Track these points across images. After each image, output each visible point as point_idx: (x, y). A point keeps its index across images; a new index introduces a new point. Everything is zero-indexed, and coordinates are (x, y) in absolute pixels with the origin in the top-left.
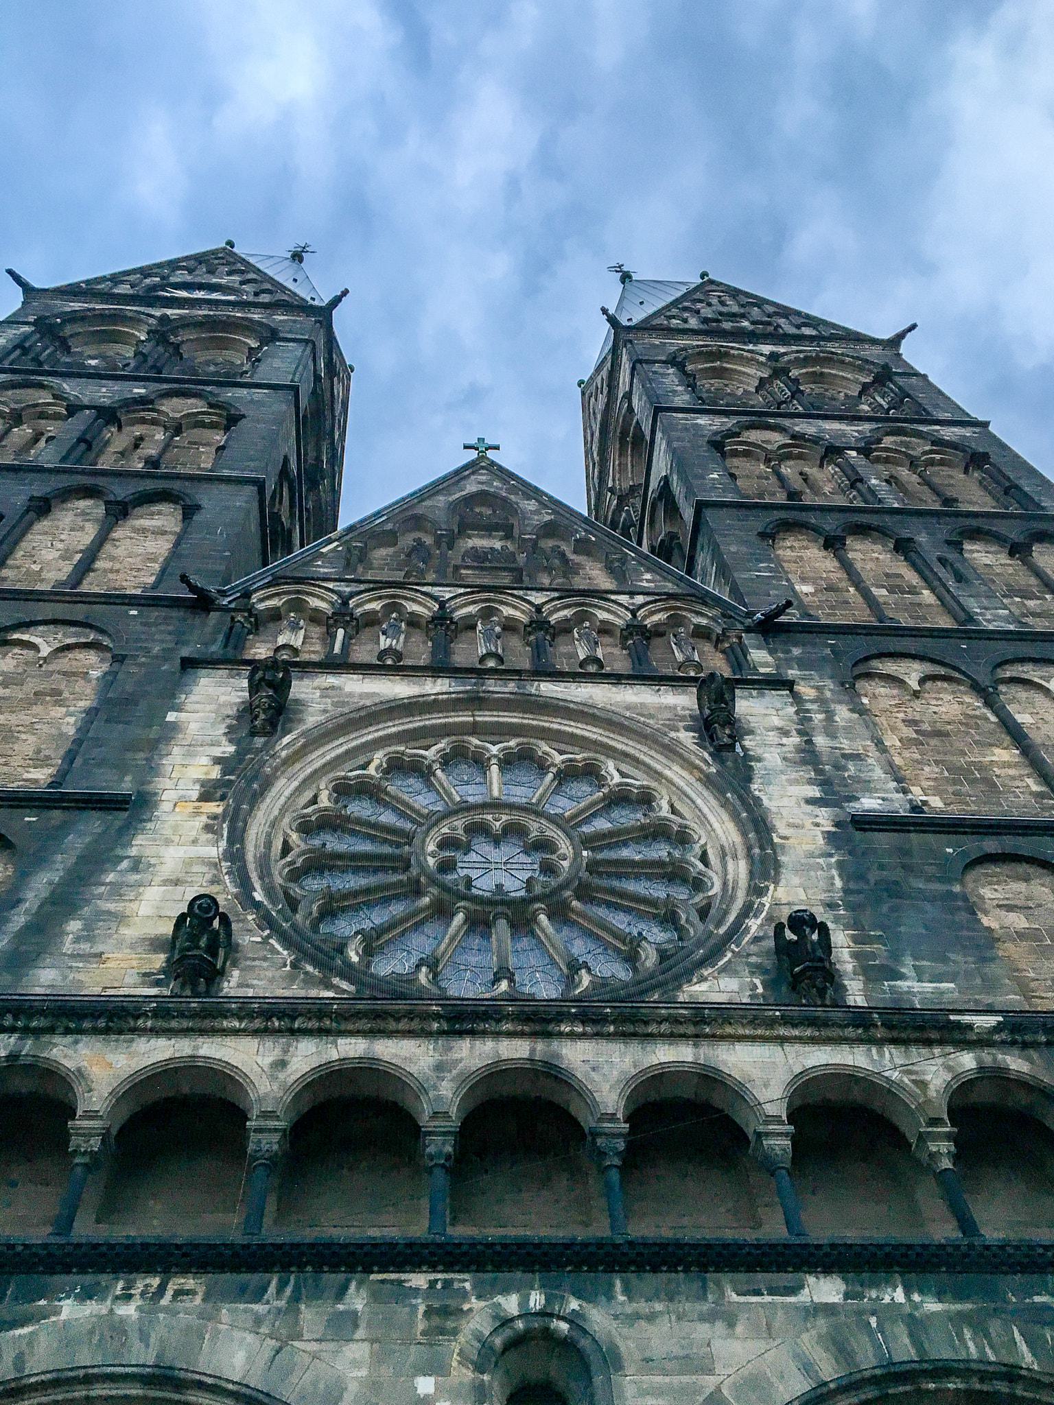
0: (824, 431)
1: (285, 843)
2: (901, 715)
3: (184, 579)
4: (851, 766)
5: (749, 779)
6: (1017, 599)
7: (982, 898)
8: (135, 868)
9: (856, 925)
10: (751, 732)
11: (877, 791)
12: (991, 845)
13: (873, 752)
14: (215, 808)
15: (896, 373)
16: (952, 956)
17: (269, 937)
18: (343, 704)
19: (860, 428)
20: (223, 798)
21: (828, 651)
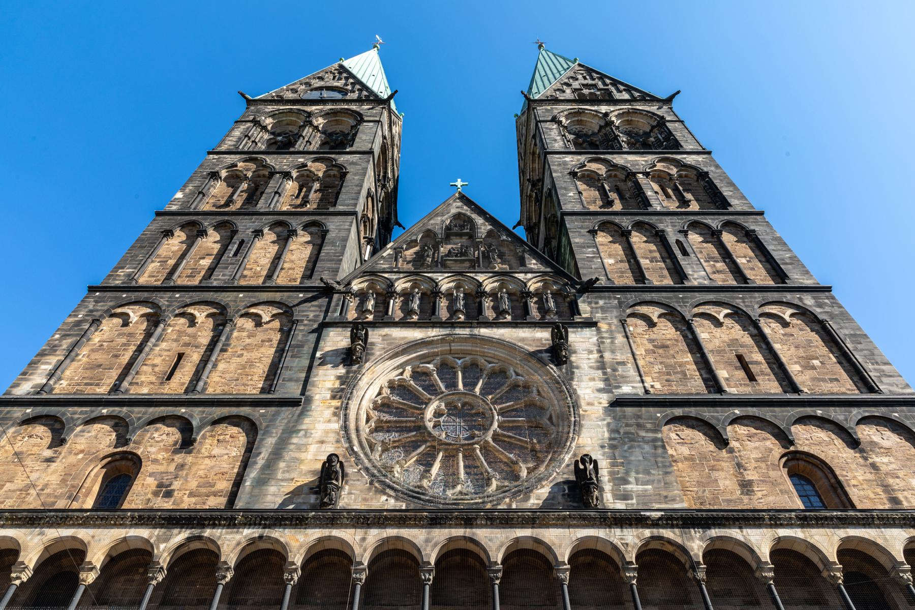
0: (628, 162)
1: (367, 415)
2: (647, 336)
3: (321, 279)
4: (620, 369)
5: (572, 379)
6: (712, 263)
7: (670, 439)
8: (305, 436)
10: (575, 352)
11: (631, 382)
14: (336, 403)
15: (669, 121)
16: (653, 472)
17: (360, 469)
18: (391, 343)
19: (646, 159)
20: (340, 398)
21: (616, 302)
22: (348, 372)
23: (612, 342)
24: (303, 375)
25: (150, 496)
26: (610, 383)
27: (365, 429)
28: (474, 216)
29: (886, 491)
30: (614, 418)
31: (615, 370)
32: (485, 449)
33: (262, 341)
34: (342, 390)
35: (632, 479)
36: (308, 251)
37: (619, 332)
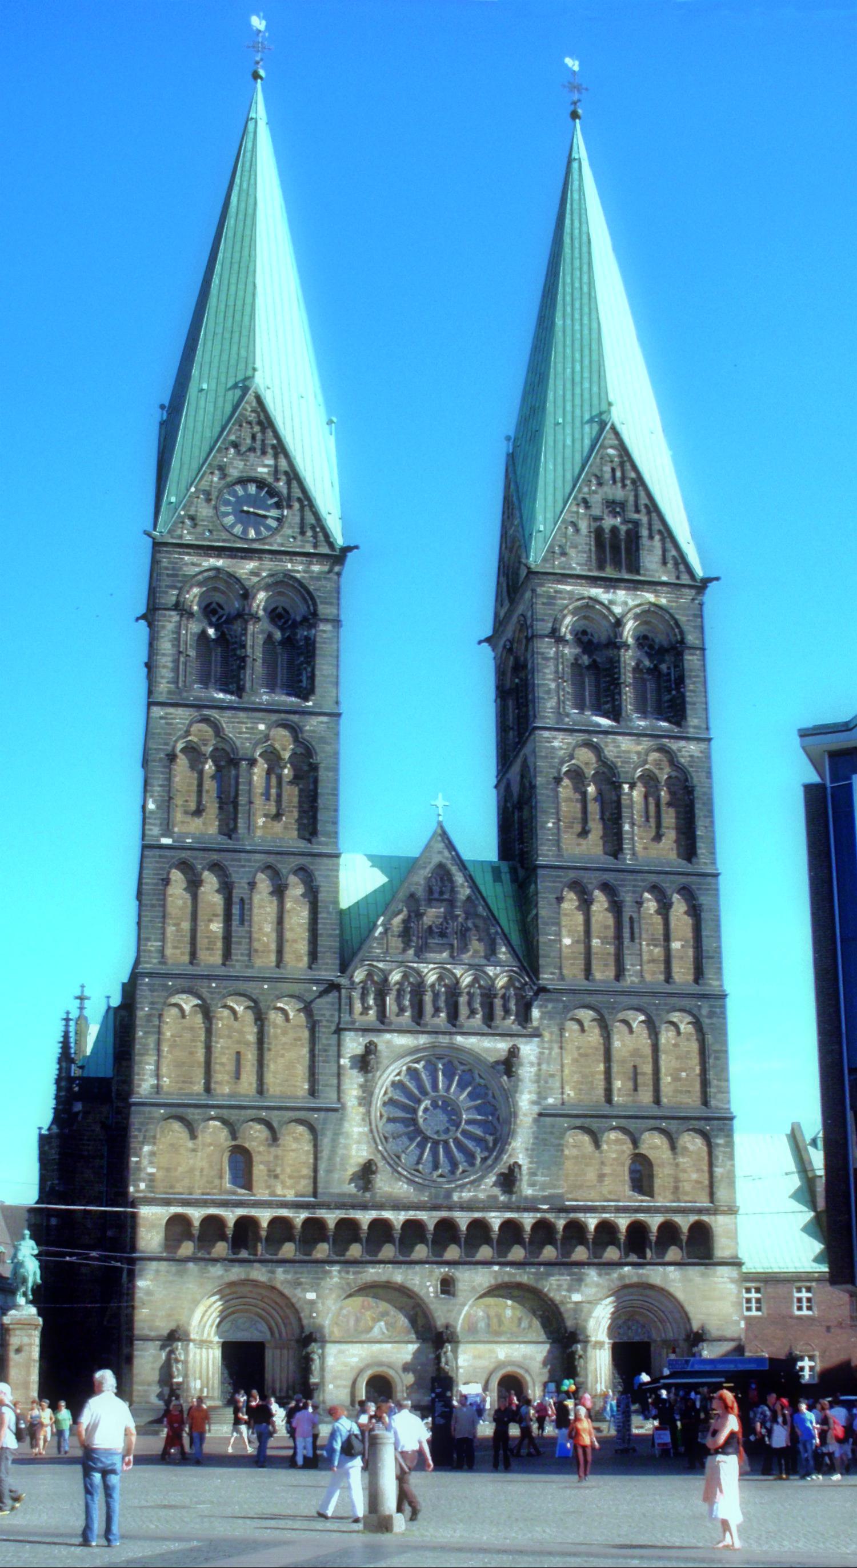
5: (516, 1092)
9: (531, 1157)
12: (578, 1122)
13: (559, 1074)
14: (362, 1110)
20: (364, 1105)
22: (366, 1081)
23: (550, 1054)
24: (335, 1081)
25: (266, 1178)
26: (541, 1096)
27: (380, 1125)
28: (454, 869)
29: (675, 1182)
30: (538, 1127)
31: (546, 1082)
32: (457, 1141)
33: (295, 1040)
34: (364, 1098)
35: (539, 1173)
36: (305, 913)
37: (556, 1042)
